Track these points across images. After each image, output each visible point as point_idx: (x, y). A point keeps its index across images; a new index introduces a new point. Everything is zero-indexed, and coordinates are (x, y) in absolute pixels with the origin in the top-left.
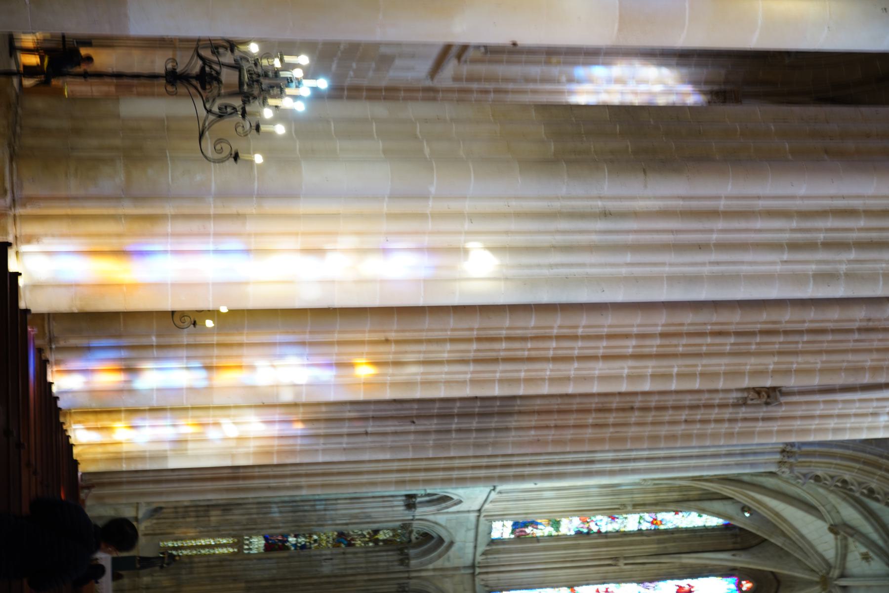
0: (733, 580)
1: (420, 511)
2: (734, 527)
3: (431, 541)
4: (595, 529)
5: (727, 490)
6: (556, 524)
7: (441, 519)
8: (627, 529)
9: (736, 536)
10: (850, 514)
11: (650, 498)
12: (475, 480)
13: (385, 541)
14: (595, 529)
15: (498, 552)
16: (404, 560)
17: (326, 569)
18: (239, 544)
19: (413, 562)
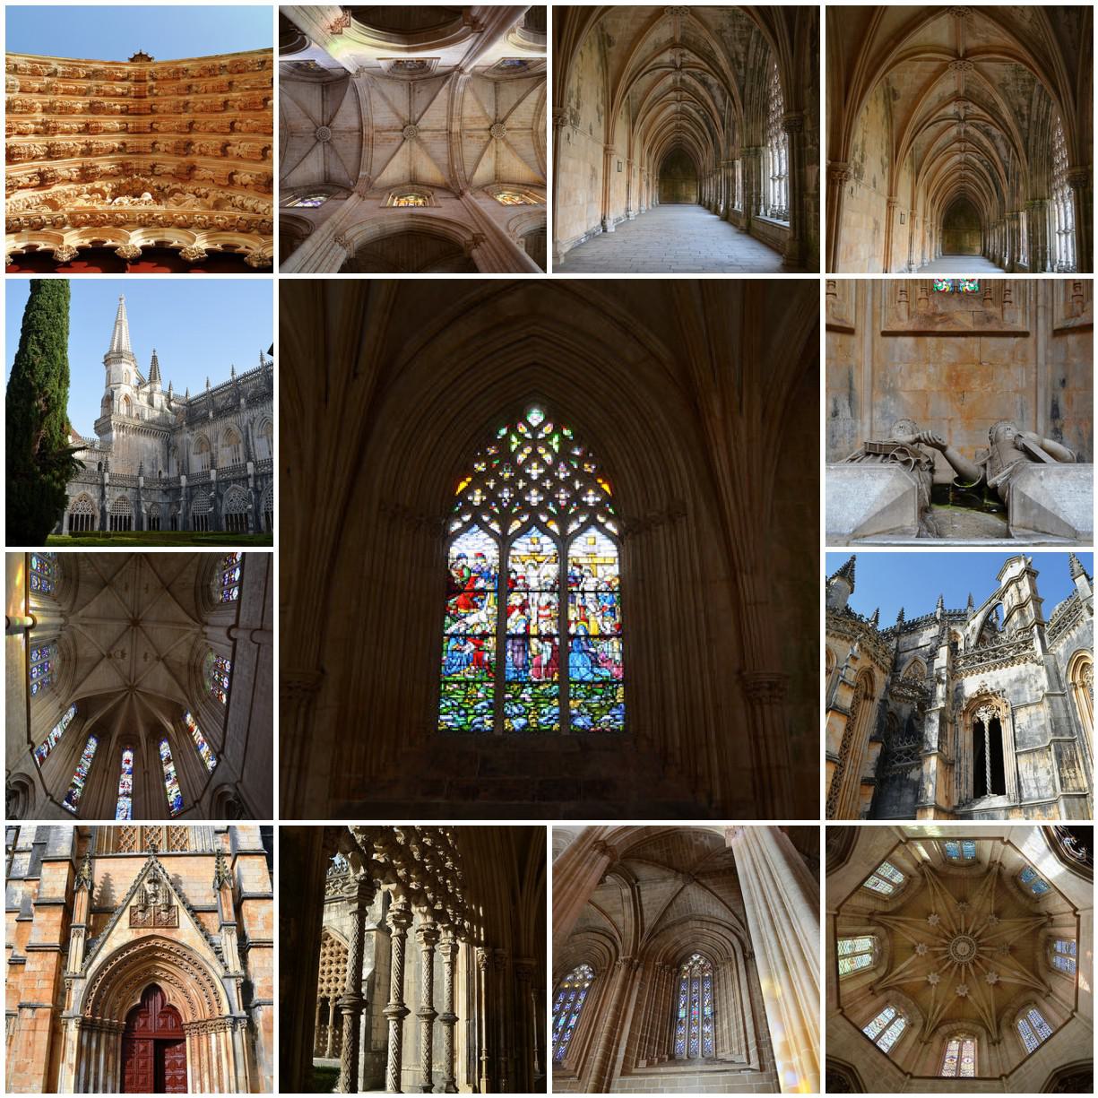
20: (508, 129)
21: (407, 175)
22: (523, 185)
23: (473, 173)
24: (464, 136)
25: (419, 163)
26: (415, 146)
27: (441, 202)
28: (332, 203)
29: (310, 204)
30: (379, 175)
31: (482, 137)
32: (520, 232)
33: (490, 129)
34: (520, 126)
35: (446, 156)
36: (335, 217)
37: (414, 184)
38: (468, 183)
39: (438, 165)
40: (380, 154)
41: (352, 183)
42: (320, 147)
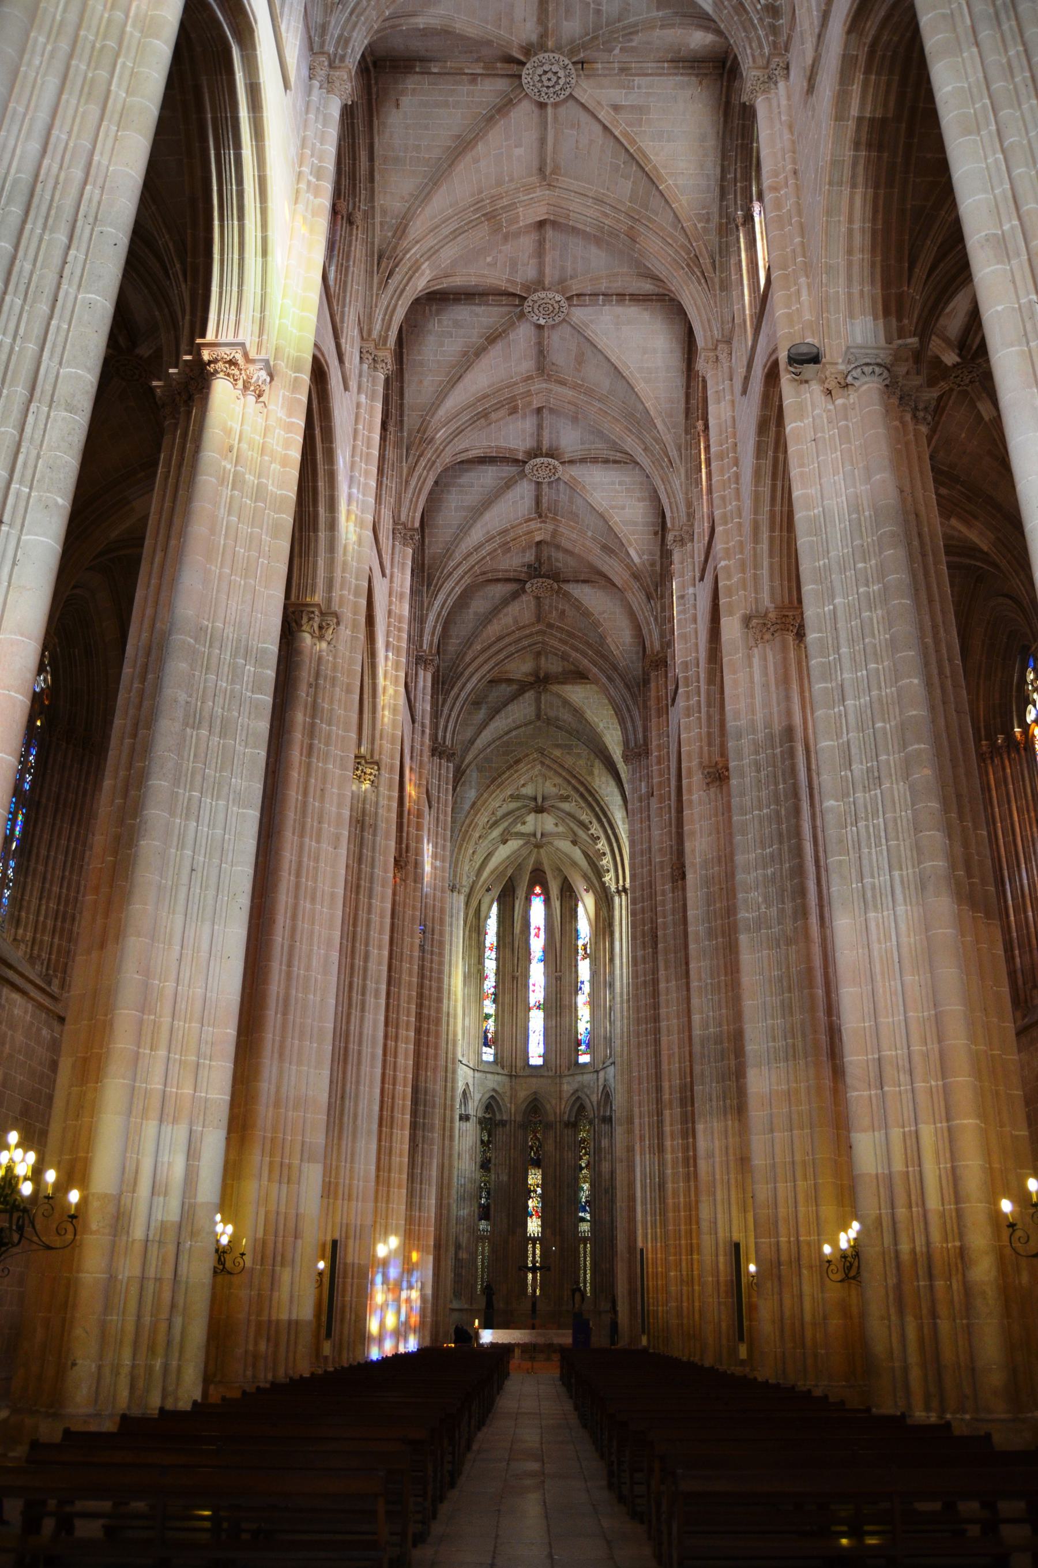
0: (533, 898)
1: (471, 1111)
2: (499, 896)
3: (491, 1105)
4: (493, 990)
5: (474, 904)
6: (487, 1017)
7: (477, 1097)
8: (495, 968)
9: (505, 896)
10: (496, 833)
11: (475, 952)
12: (454, 1072)
13: (489, 1136)
14: (493, 990)
15: (502, 1058)
16: (503, 1123)
17: (504, 1178)
18: (482, 1238)
19: (505, 1118)
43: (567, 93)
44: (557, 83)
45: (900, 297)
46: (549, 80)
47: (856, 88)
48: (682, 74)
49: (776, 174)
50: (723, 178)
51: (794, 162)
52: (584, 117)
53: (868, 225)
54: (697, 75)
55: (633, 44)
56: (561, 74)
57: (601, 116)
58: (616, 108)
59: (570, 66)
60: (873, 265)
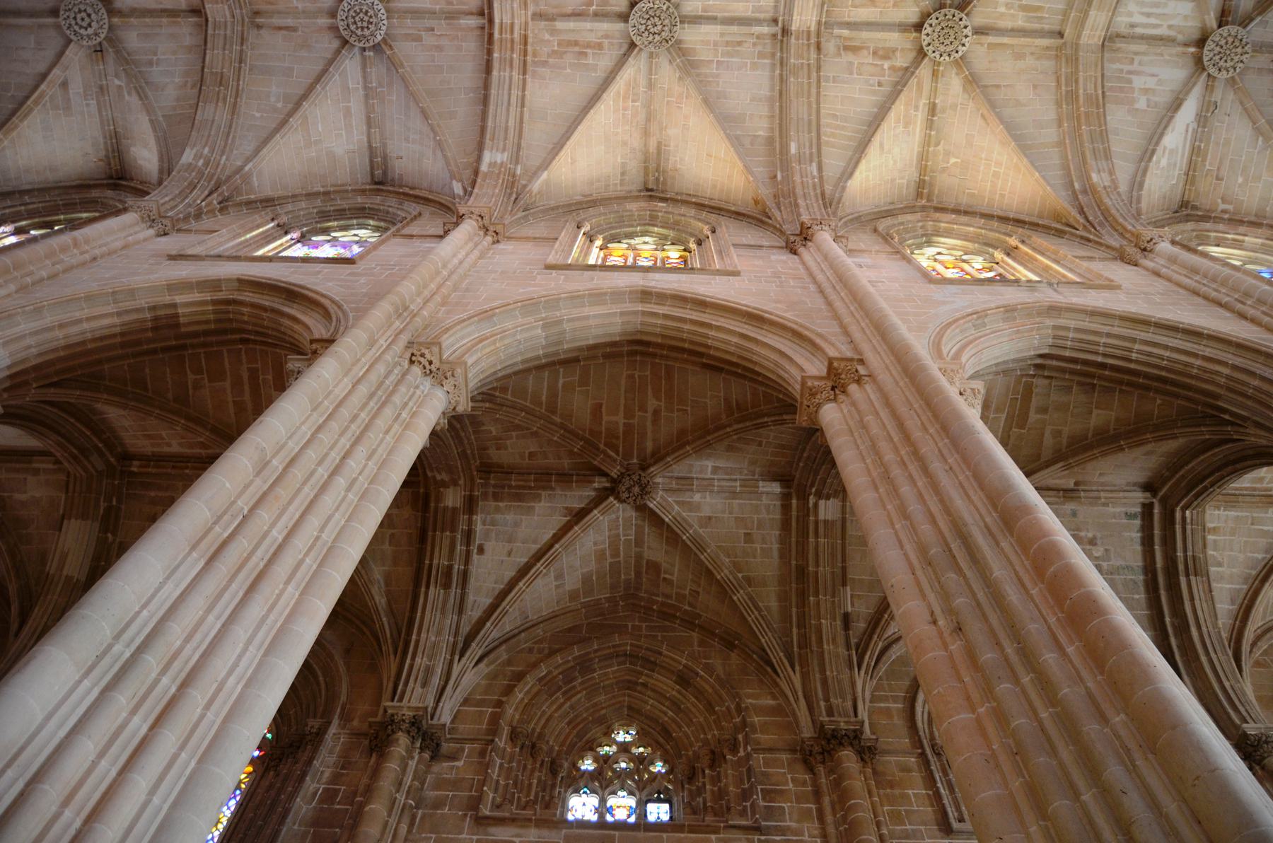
20: (979, 31)
21: (634, 167)
22: (1004, 219)
23: (849, 173)
24: (830, 46)
25: (672, 132)
26: (667, 73)
27: (737, 259)
28: (396, 249)
29: (327, 251)
30: (545, 165)
31: (887, 54)
32: (971, 362)
33: (918, 27)
34: (1020, 23)
35: (764, 110)
36: (407, 288)
37: (655, 195)
38: (829, 202)
39: (735, 141)
40: (549, 93)
41: (458, 188)
42: (350, 65)
43: (72, 37)
44: (81, 27)
45: (26, 383)
46: (83, 19)
47: (196, 296)
48: (105, 143)
49: (87, 242)
50: (22, 193)
51: (102, 256)
52: (50, 54)
53: (89, 336)
54: (107, 156)
55: (127, 97)
56: (90, 31)
57: (56, 71)
58: (65, 85)
59: (99, 40)
60: (55, 350)
